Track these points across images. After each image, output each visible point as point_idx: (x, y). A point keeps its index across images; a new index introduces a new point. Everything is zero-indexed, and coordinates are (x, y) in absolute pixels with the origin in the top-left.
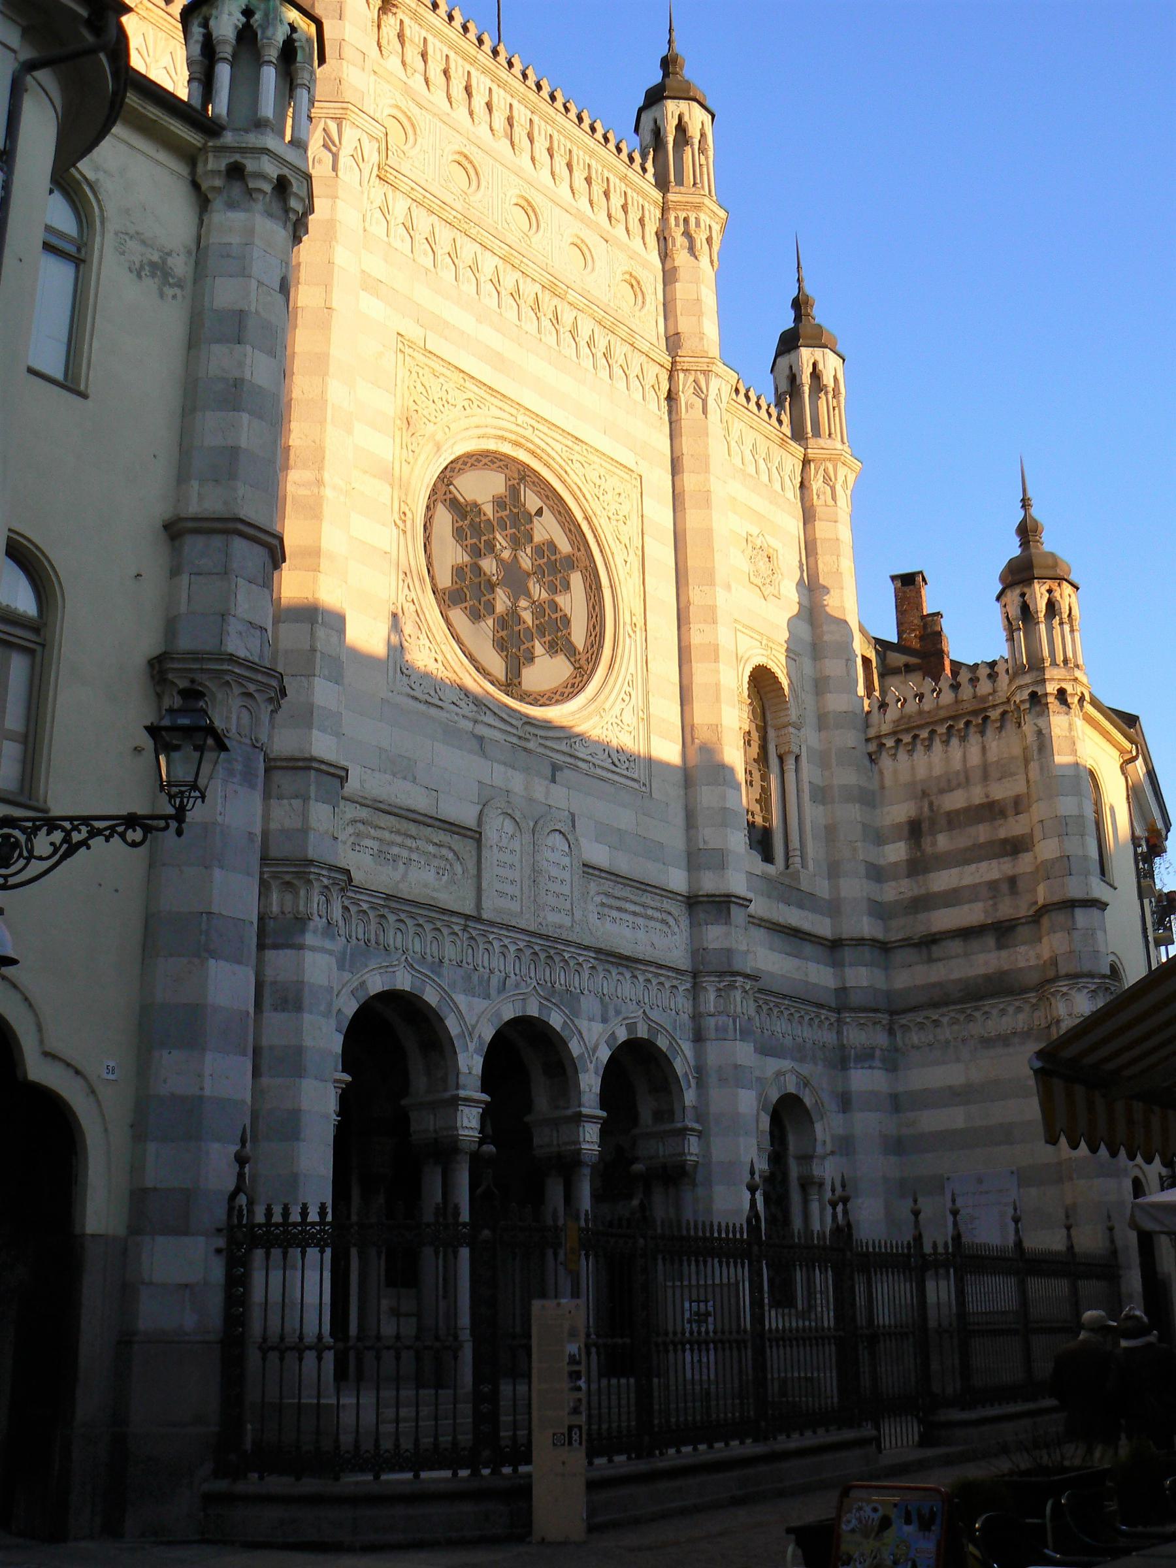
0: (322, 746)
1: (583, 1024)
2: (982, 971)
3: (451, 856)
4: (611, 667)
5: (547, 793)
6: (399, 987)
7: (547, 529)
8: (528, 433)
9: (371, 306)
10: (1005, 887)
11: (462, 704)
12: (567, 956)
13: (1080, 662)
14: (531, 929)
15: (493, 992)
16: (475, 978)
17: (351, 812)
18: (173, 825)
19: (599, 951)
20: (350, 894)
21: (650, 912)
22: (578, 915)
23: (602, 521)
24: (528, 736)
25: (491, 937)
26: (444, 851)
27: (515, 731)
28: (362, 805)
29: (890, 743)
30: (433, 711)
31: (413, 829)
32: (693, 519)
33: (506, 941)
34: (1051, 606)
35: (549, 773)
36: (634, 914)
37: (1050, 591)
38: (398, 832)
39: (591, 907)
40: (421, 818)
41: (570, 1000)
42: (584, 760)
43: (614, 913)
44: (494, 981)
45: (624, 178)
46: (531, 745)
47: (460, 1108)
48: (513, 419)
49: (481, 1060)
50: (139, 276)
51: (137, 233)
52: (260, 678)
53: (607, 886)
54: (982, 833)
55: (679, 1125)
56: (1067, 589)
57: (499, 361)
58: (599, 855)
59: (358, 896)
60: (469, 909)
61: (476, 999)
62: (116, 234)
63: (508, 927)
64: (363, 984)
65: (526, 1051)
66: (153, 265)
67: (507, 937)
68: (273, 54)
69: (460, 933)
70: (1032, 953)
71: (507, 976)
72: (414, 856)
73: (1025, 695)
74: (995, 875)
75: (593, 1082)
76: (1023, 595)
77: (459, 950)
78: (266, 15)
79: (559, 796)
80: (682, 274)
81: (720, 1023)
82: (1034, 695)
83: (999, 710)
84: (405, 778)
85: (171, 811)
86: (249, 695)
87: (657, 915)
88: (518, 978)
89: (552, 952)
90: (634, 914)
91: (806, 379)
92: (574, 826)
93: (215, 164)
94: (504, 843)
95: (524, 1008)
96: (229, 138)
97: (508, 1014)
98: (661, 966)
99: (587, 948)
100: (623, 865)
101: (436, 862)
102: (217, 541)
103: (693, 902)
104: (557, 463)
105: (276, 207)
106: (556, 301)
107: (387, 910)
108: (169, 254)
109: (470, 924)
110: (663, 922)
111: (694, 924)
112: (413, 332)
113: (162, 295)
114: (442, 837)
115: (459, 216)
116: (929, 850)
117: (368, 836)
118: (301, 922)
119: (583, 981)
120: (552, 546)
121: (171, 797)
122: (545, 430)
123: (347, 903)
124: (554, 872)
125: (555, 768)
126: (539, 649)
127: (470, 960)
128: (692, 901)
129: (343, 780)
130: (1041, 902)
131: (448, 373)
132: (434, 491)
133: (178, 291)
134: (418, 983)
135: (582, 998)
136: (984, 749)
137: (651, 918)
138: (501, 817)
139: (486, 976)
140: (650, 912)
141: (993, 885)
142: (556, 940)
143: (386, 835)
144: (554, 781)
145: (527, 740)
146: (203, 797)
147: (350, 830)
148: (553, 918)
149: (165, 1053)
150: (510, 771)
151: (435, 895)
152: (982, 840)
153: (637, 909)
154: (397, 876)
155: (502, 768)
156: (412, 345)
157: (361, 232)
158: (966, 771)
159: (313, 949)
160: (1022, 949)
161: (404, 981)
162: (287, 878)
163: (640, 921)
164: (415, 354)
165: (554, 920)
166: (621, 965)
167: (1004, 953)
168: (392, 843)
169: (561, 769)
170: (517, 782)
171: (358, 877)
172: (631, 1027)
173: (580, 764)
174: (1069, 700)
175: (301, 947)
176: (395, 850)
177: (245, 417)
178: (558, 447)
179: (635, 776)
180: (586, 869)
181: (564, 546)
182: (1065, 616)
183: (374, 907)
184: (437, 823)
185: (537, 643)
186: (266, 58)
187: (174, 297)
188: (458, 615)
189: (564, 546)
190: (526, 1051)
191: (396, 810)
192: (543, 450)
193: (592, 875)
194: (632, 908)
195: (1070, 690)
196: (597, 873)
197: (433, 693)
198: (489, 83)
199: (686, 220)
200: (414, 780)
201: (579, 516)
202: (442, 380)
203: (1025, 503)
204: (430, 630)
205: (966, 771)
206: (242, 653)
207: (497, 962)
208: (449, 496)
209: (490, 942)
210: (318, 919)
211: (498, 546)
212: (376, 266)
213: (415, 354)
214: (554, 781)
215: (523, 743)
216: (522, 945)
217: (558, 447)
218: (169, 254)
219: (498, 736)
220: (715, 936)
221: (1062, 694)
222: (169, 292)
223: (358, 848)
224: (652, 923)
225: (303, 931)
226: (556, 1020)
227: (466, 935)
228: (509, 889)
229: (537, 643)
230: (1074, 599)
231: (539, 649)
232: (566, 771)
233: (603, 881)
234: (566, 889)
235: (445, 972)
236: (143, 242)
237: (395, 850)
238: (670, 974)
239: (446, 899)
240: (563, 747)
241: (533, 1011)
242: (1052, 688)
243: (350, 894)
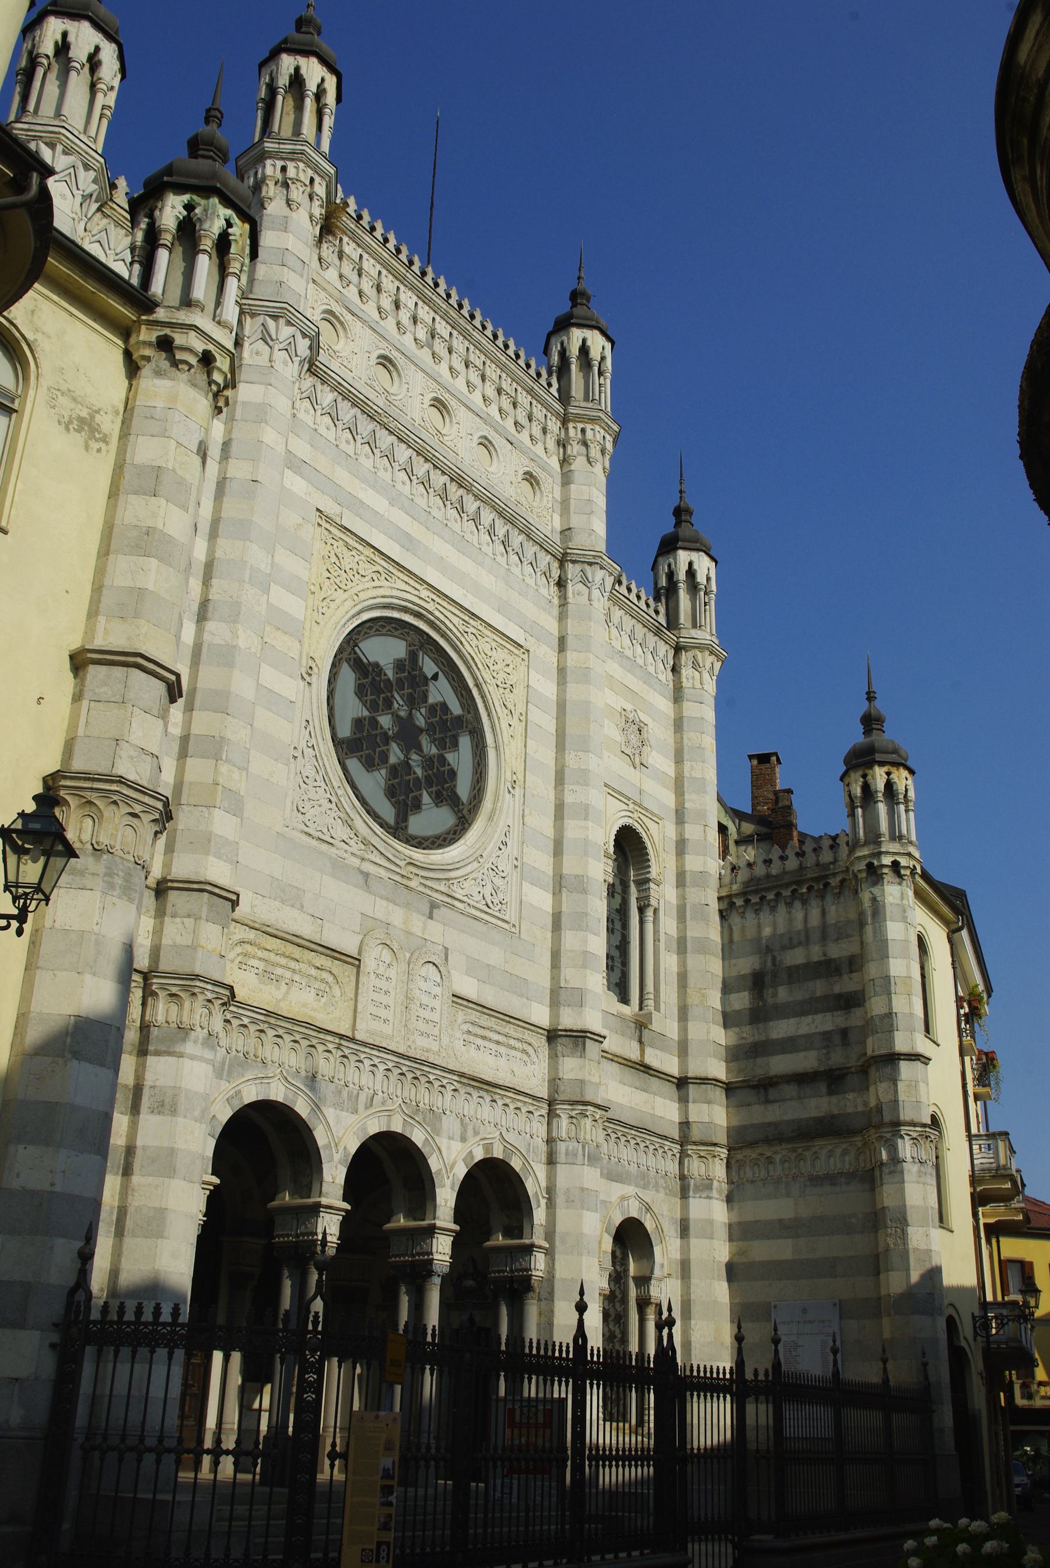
0: (218, 872)
1: (443, 1142)
2: (814, 1114)
3: (330, 979)
4: (490, 818)
5: (424, 929)
6: (273, 1098)
7: (441, 692)
8: (430, 607)
9: (296, 484)
10: (837, 1039)
11: (352, 842)
12: (432, 1077)
13: (914, 838)
14: (401, 1051)
15: (361, 1107)
16: (345, 1093)
17: (240, 933)
18: (15, 924)
19: (462, 1075)
20: (232, 1008)
21: (512, 1042)
22: (445, 1040)
23: (491, 689)
24: (411, 876)
25: (363, 1056)
26: (325, 975)
27: (398, 870)
29: (739, 902)
30: (324, 847)
31: (297, 952)
32: (573, 691)
34: (889, 786)
35: (426, 908)
36: (498, 1043)
37: (888, 774)
38: (283, 955)
39: (458, 1034)
41: (432, 1118)
42: (460, 901)
43: (479, 1042)
44: (363, 1098)
45: (530, 391)
46: (413, 884)
47: (322, 1214)
48: (416, 593)
49: (345, 1170)
50: (67, 429)
51: (69, 390)
52: (146, 799)
53: (474, 1016)
54: (819, 987)
55: (527, 1241)
56: (904, 773)
57: (408, 542)
58: (469, 988)
59: (241, 1011)
60: (344, 1029)
61: (344, 1113)
62: (49, 389)
63: (379, 1048)
64: (238, 1093)
65: (389, 1167)
66: (81, 420)
68: (207, 244)
69: (334, 1051)
70: (859, 1100)
71: (375, 1093)
72: (297, 978)
73: (862, 865)
74: (828, 1027)
75: (449, 1197)
76: (864, 776)
77: (332, 1067)
78: (206, 210)
79: (435, 931)
80: (577, 477)
81: (571, 1148)
82: (870, 866)
83: (839, 878)
84: (293, 906)
85: (16, 912)
86: (135, 815)
87: (518, 1045)
88: (386, 1095)
89: (418, 1073)
90: (498, 1043)
91: (682, 576)
92: (446, 959)
93: (147, 335)
94: (381, 971)
95: (389, 1123)
96: (161, 314)
97: (374, 1129)
99: (451, 1072)
101: (317, 985)
102: (118, 672)
103: (552, 1036)
104: (454, 635)
105: (201, 378)
106: (461, 491)
107: (266, 1025)
108: (98, 412)
109: (343, 1042)
110: (524, 1051)
111: (553, 1057)
112: (331, 508)
113: (87, 448)
115: (380, 411)
116: (770, 1001)
118: (184, 1031)
119: (446, 1101)
120: (444, 706)
121: (15, 899)
122: (445, 604)
123: (229, 1016)
124: (425, 999)
125: (433, 906)
126: (426, 798)
127: (341, 1076)
128: (553, 1034)
129: (235, 904)
130: (869, 1052)
131: (360, 548)
132: (341, 650)
133: (102, 445)
134: (291, 1095)
136: (824, 913)
137: (514, 1048)
139: (355, 1092)
140: (512, 1042)
141: (826, 1036)
142: (423, 1062)
143: (272, 957)
144: (431, 917)
145: (409, 879)
146: (47, 899)
147: (239, 949)
148: (421, 1042)
149: (21, 1147)
150: (391, 906)
151: (313, 1014)
152: (818, 994)
153: (501, 1038)
154: (279, 994)
155: (384, 903)
156: (329, 519)
157: (289, 416)
158: (807, 930)
159: (193, 1058)
160: (851, 1096)
161: (277, 1093)
162: (174, 990)
163: (502, 1050)
164: (332, 529)
165: (421, 1046)
166: (482, 1089)
167: (834, 1099)
169: (438, 907)
170: (397, 916)
171: (241, 994)
172: (488, 1147)
173: (456, 903)
174: (903, 872)
175: (181, 1055)
176: (279, 971)
177: (154, 562)
178: (455, 620)
179: (507, 918)
180: (455, 999)
181: (456, 708)
182: (901, 796)
185: (425, 794)
186: (202, 247)
187: (99, 450)
188: (353, 764)
189: (456, 709)
190: (389, 1167)
192: (441, 622)
194: (496, 1037)
195: (903, 861)
196: (465, 1003)
197: (325, 830)
198: (415, 299)
199: (583, 431)
200: (302, 908)
201: (471, 683)
202: (354, 553)
203: (870, 697)
204: (327, 774)
205: (807, 930)
206: (132, 776)
207: (366, 1080)
208: (353, 656)
210: (199, 1029)
211: (396, 705)
212: (301, 448)
213: (332, 529)
214: (431, 917)
215: (405, 881)
216: (390, 1065)
217: (455, 620)
218: (98, 412)
219: (383, 873)
220: (570, 1067)
221: (895, 865)
222: (95, 445)
223: (244, 967)
224: (513, 1053)
225: (184, 1040)
226: (418, 1137)
227: (340, 1053)
228: (382, 1013)
229: (425, 794)
230: (910, 782)
231: (426, 798)
232: (443, 909)
233: (470, 1011)
234: (435, 1017)
236: (74, 399)
237: (279, 971)
238: (527, 1100)
239: (322, 1019)
240: (442, 887)
241: (397, 1127)
242: (887, 860)
243: (232, 1008)
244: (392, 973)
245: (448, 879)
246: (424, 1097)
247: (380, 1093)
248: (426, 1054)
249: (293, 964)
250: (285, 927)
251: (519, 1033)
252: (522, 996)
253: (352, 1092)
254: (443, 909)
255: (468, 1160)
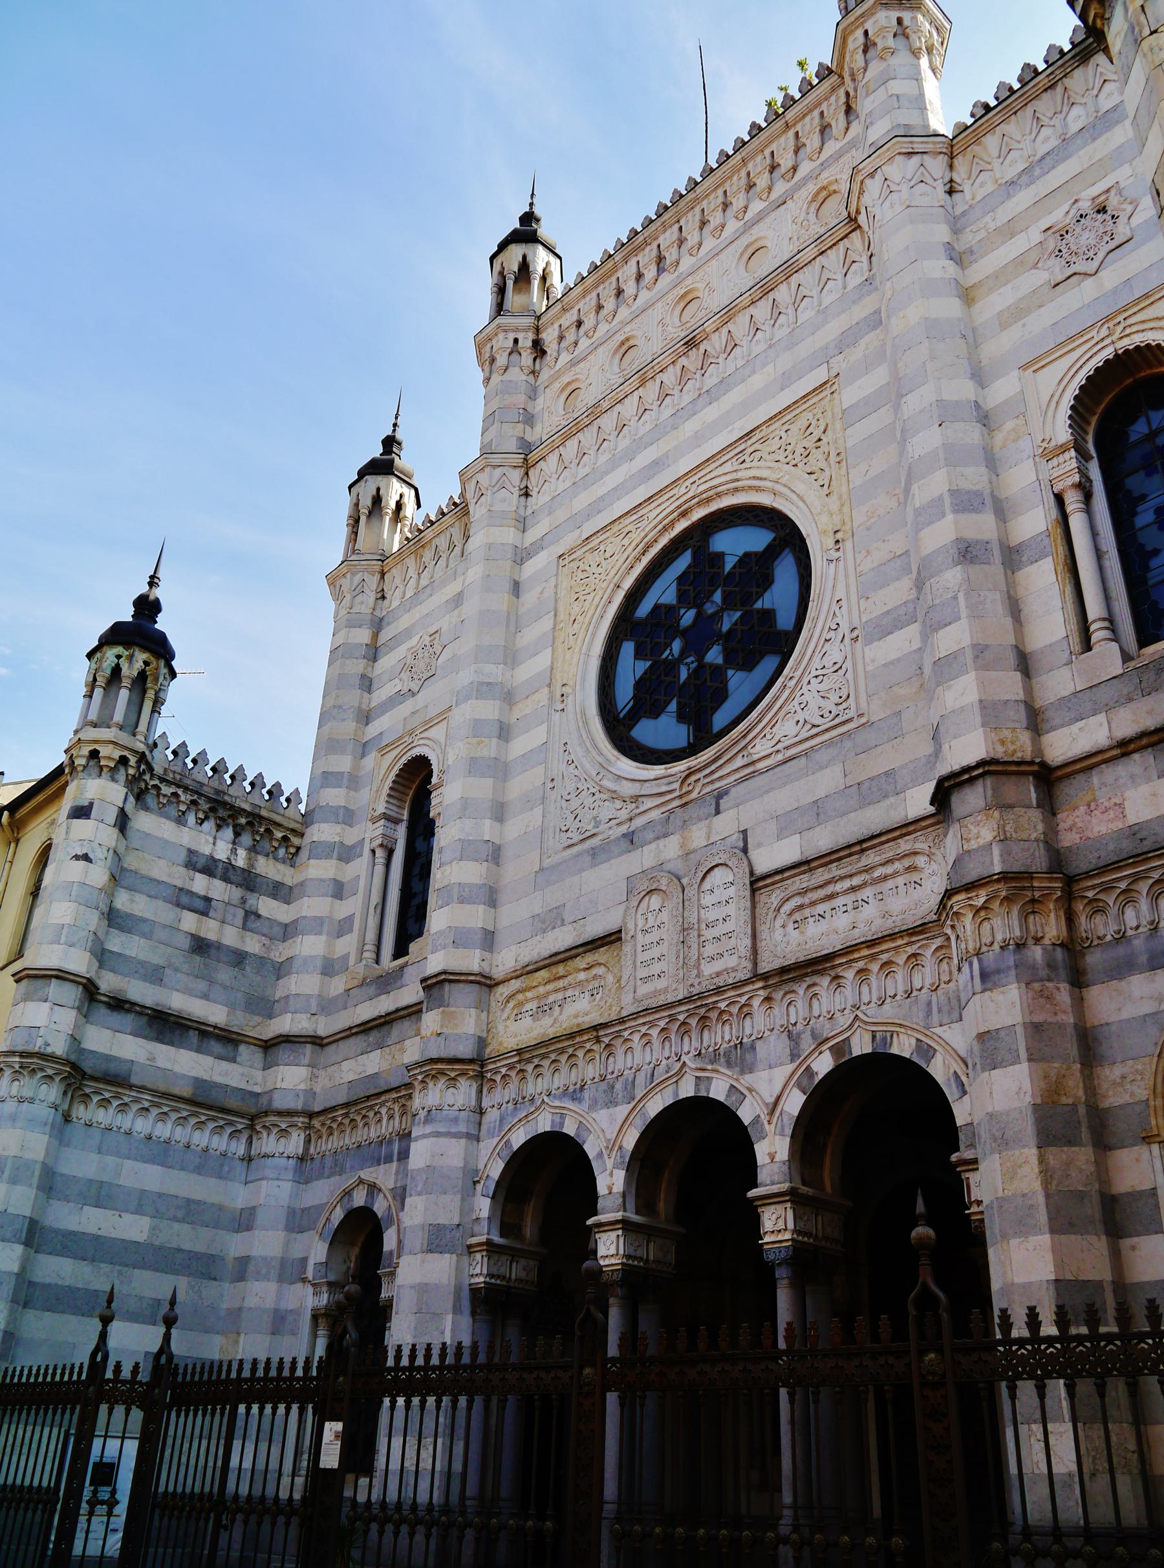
12: (722, 1005)
24: (691, 788)
25: (626, 1034)
26: (594, 971)
28: (517, 977)
31: (560, 969)
33: (643, 1029)
36: (853, 889)
40: (567, 954)
43: (820, 909)
46: (694, 795)
57: (657, 465)
67: (644, 1024)
69: (595, 1047)
72: (569, 993)
75: (778, 1147)
87: (889, 870)
89: (703, 1011)
90: (853, 889)
98: (872, 943)
100: (824, 839)
104: (727, 483)
109: (601, 1033)
114: (590, 958)
117: (527, 1001)
124: (710, 915)
135: (758, 1044)
137: (885, 878)
138: (647, 898)
147: (511, 1005)
153: (856, 881)
163: (868, 893)
166: (806, 975)
168: (548, 993)
169: (727, 793)
176: (551, 999)
183: (511, 1067)
184: (580, 950)
191: (542, 964)
193: (773, 884)
194: (847, 884)
209: (627, 1040)
235: (586, 1094)
237: (551, 999)
238: (900, 942)
244: (664, 916)
245: (745, 747)
246: (721, 1036)
247: (664, 1062)
248: (715, 980)
249: (560, 984)
250: (546, 954)
251: (889, 851)
252: (886, 796)
253: (627, 1080)
254: (733, 790)
255: (805, 1082)
